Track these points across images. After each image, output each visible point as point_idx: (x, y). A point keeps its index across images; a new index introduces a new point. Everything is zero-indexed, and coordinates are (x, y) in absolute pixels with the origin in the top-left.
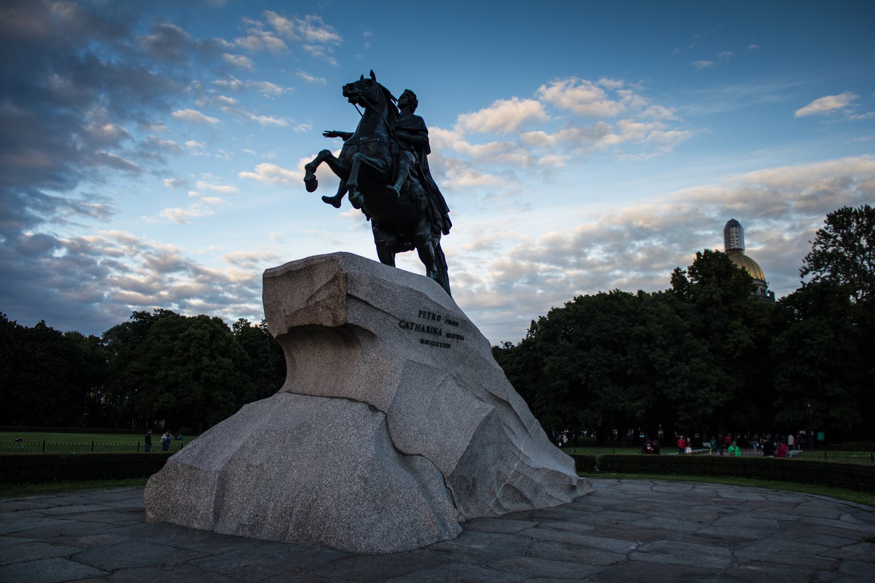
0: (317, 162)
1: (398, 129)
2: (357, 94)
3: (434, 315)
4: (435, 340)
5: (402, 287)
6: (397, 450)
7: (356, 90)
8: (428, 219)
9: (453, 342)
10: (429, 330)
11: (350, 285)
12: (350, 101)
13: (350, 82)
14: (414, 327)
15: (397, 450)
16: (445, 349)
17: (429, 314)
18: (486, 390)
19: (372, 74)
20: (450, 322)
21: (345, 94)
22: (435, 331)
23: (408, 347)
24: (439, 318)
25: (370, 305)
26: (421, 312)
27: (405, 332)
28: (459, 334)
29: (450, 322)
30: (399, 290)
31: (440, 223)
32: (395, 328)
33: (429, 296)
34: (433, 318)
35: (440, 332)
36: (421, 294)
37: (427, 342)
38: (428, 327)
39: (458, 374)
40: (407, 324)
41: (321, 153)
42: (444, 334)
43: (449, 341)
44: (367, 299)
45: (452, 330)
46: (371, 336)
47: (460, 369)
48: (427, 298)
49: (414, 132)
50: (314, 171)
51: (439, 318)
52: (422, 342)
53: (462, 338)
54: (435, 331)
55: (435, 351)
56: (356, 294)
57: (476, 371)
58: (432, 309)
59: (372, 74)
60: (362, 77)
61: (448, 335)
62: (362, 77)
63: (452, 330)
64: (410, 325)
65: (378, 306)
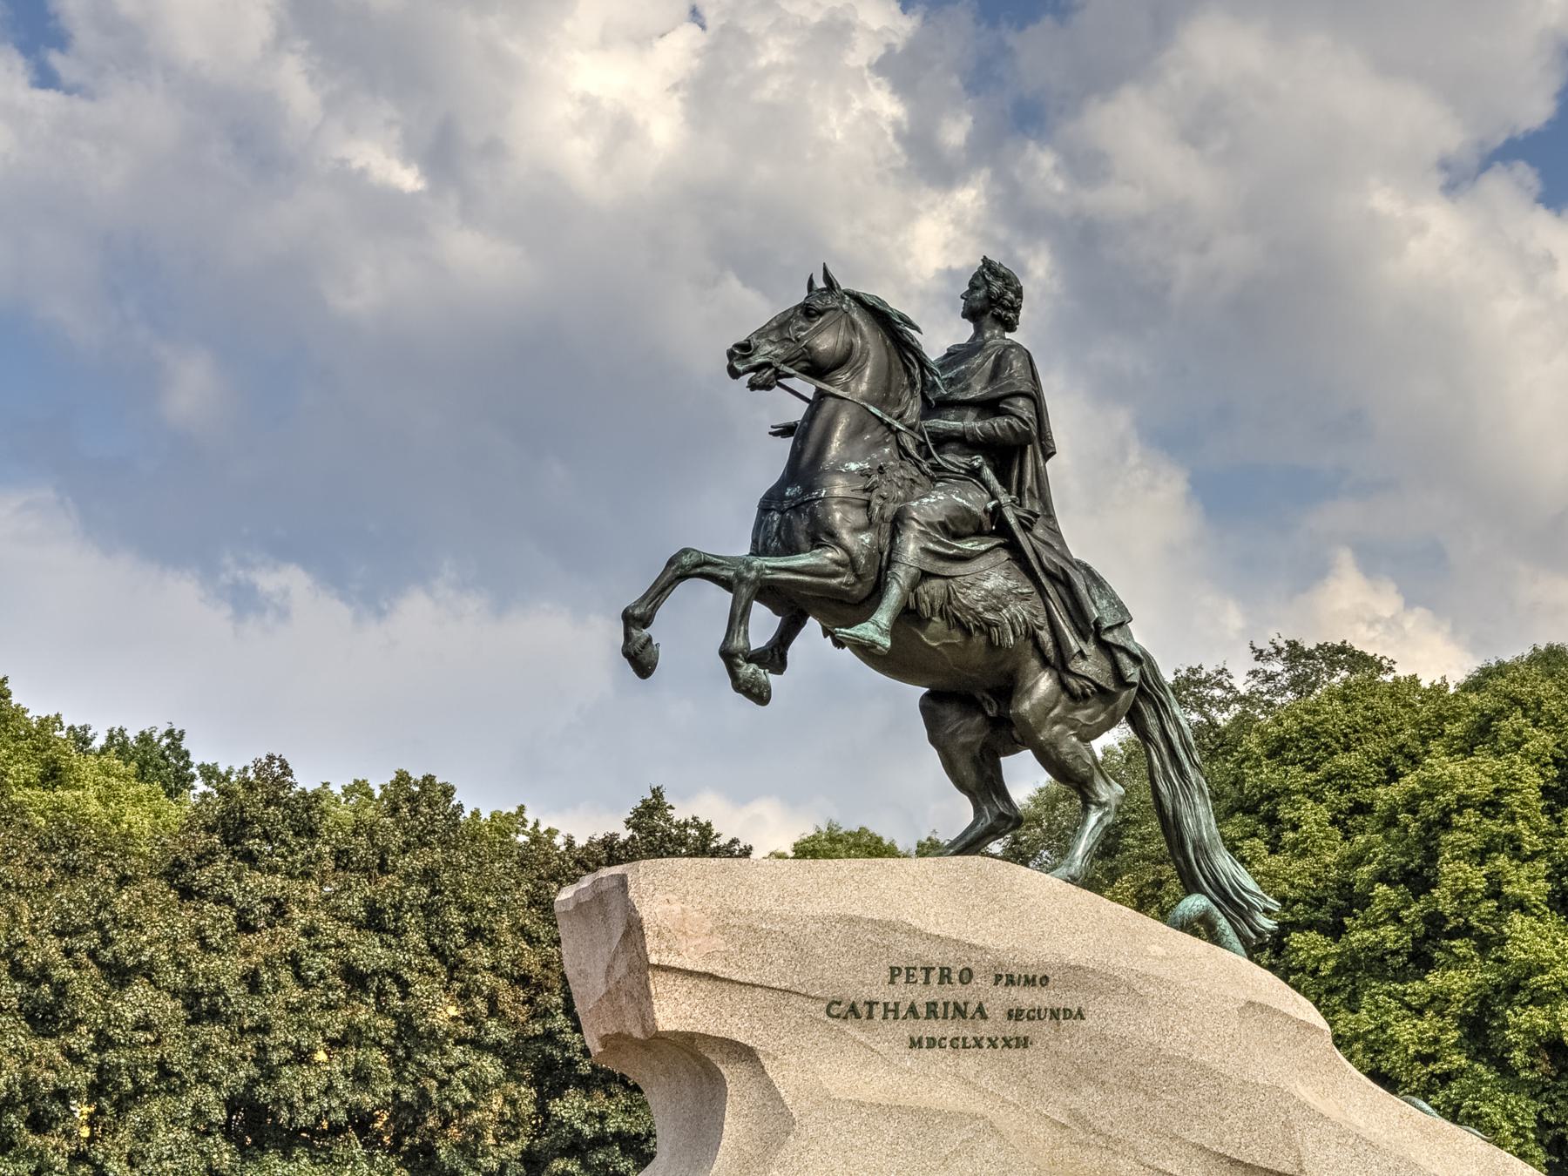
0: (660, 591)
1: (933, 407)
2: (768, 365)
3: (945, 975)
4: (969, 1034)
5: (823, 920)
7: (766, 351)
8: (1046, 663)
11: (651, 943)
12: (753, 386)
13: (741, 339)
14: (878, 1011)
16: (1014, 1054)
17: (928, 970)
18: (1202, 1148)
19: (828, 278)
21: (735, 374)
22: (960, 1011)
23: (865, 1065)
24: (967, 976)
25: (723, 980)
26: (894, 972)
27: (851, 1028)
28: (1061, 1004)
29: (1011, 981)
30: (812, 927)
31: (1091, 666)
32: (819, 1021)
33: (916, 923)
34: (945, 975)
35: (980, 1009)
36: (890, 926)
37: (932, 1043)
38: (932, 1008)
39: (1075, 1115)
40: (853, 1008)
41: (671, 563)
42: (996, 1011)
43: (1023, 1028)
44: (716, 967)
45: (1026, 998)
46: (744, 1054)
47: (1087, 1099)
48: (912, 932)
49: (989, 407)
50: (645, 621)
51: (967, 976)
52: (915, 1043)
53: (1080, 1015)
54: (960, 1011)
55: (969, 1062)
56: (675, 962)
57: (1152, 1098)
58: (935, 957)
59: (828, 278)
60: (811, 282)
61: (1015, 1015)
62: (811, 282)
63: (1026, 998)
64: (863, 1010)
65: (750, 978)
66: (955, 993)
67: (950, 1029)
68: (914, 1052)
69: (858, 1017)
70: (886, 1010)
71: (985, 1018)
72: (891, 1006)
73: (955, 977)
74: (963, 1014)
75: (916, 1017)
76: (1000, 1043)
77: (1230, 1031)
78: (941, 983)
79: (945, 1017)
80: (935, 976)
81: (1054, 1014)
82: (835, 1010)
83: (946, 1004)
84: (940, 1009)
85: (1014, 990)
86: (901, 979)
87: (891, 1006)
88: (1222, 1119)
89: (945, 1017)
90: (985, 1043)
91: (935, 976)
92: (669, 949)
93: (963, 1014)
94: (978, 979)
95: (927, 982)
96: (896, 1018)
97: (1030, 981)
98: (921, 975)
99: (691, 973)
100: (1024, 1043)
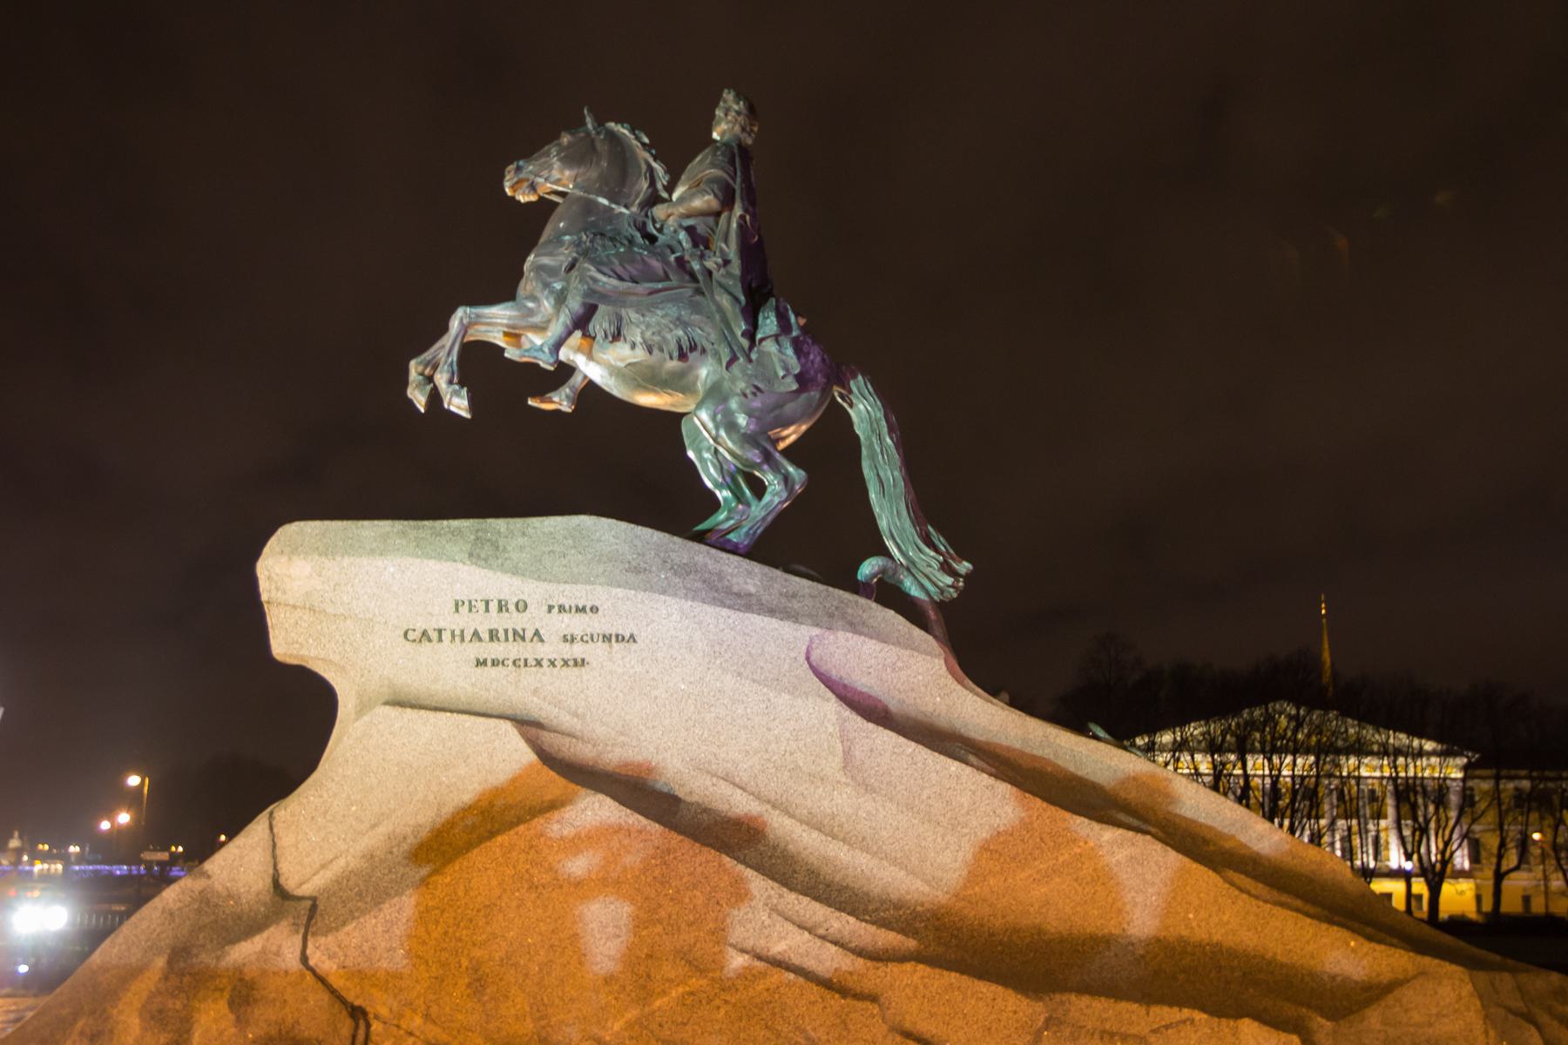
3: (502, 607)
6: (276, 884)
9: (595, 652)
10: (493, 635)
14: (446, 636)
15: (276, 884)
20: (562, 609)
22: (519, 636)
24: (522, 606)
29: (562, 609)
34: (502, 607)
35: (537, 633)
37: (495, 663)
38: (493, 635)
40: (424, 633)
51: (522, 606)
52: (481, 663)
54: (519, 636)
61: (569, 639)
66: (514, 620)
67: (512, 650)
68: (480, 670)
69: (430, 640)
70: (453, 636)
71: (542, 641)
72: (457, 632)
73: (512, 607)
74: (523, 639)
75: (480, 640)
76: (559, 663)
77: (793, 655)
78: (500, 610)
79: (507, 639)
80: (494, 606)
81: (607, 638)
82: (411, 635)
83: (506, 631)
84: (501, 635)
85: (566, 616)
86: (464, 609)
87: (457, 632)
88: (769, 729)
89: (507, 639)
90: (545, 663)
91: (494, 606)
92: (277, 589)
93: (523, 639)
94: (531, 608)
95: (487, 610)
96: (463, 640)
97: (583, 610)
98: (482, 606)
99: (295, 607)
100: (580, 663)
